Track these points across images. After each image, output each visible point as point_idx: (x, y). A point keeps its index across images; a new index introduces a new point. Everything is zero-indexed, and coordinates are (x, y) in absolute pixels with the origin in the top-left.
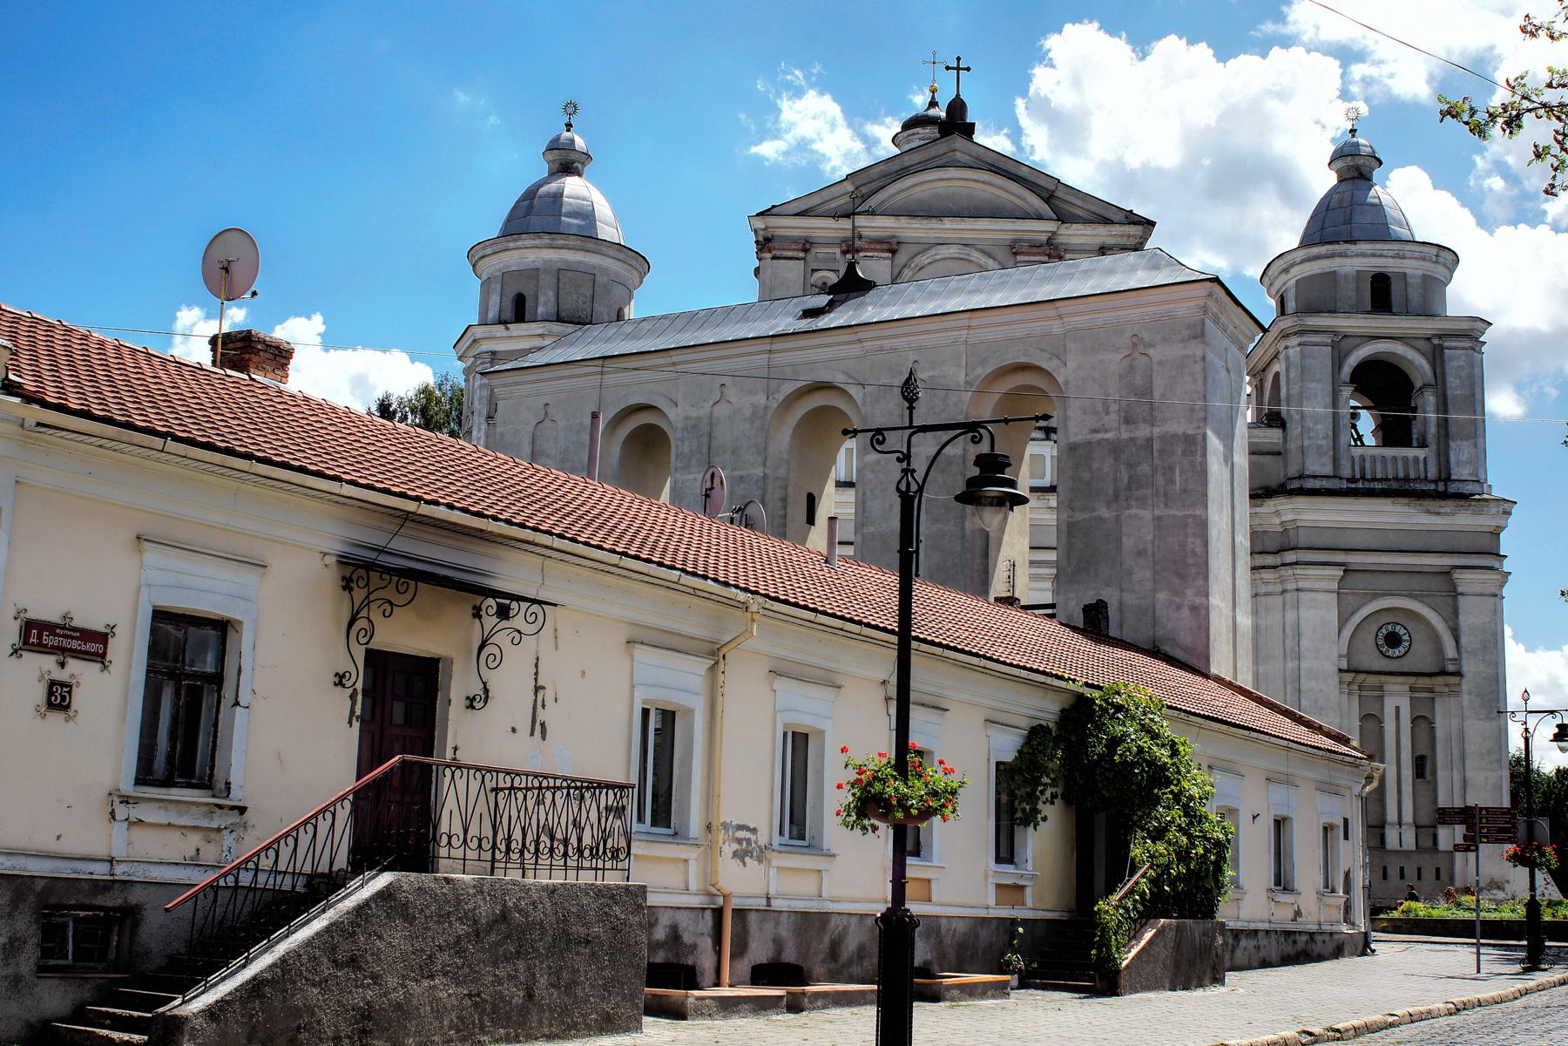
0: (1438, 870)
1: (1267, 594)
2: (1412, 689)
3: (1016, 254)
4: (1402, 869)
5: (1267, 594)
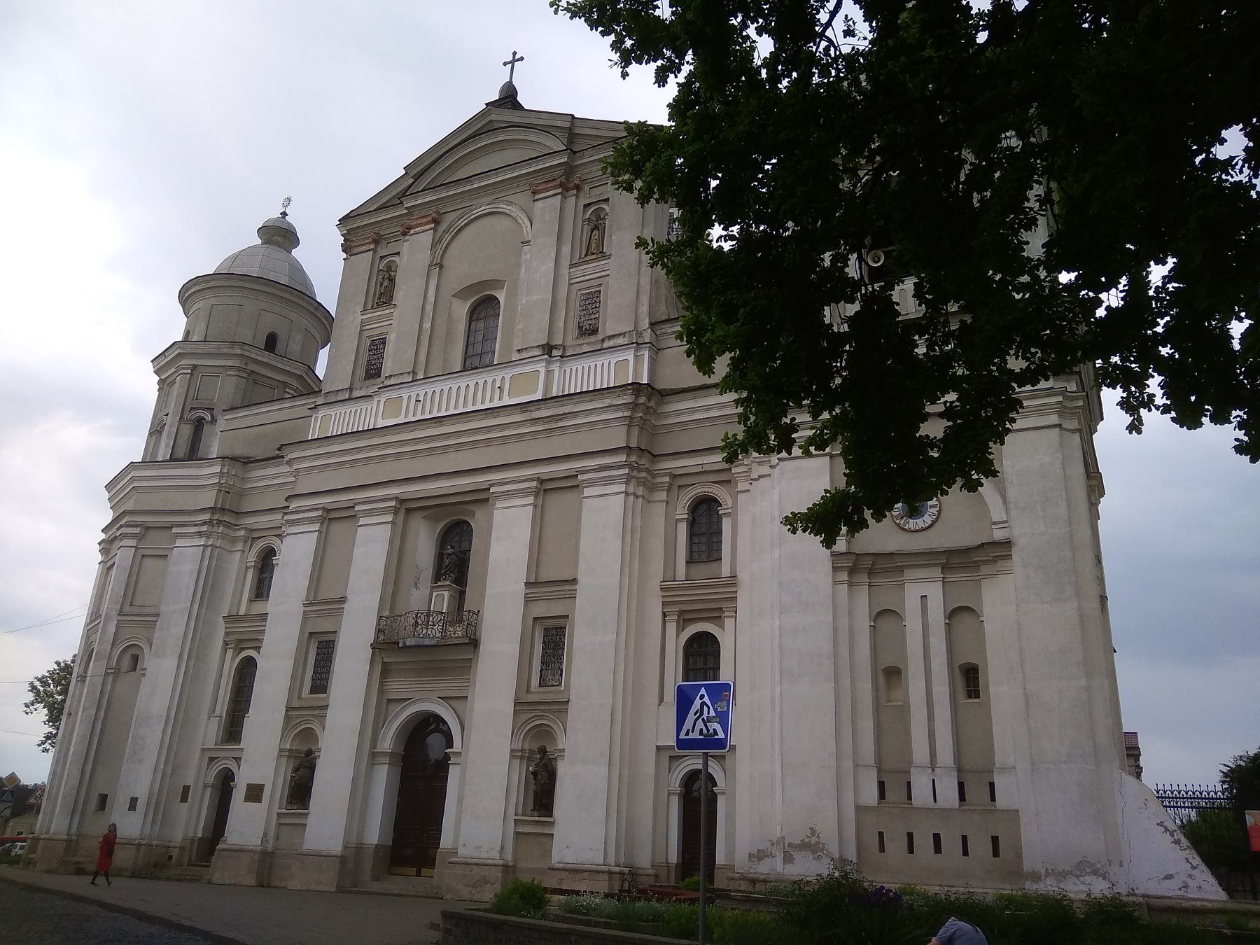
0: (995, 840)
1: (761, 477)
2: (944, 568)
3: (535, 193)
4: (937, 837)
5: (761, 477)
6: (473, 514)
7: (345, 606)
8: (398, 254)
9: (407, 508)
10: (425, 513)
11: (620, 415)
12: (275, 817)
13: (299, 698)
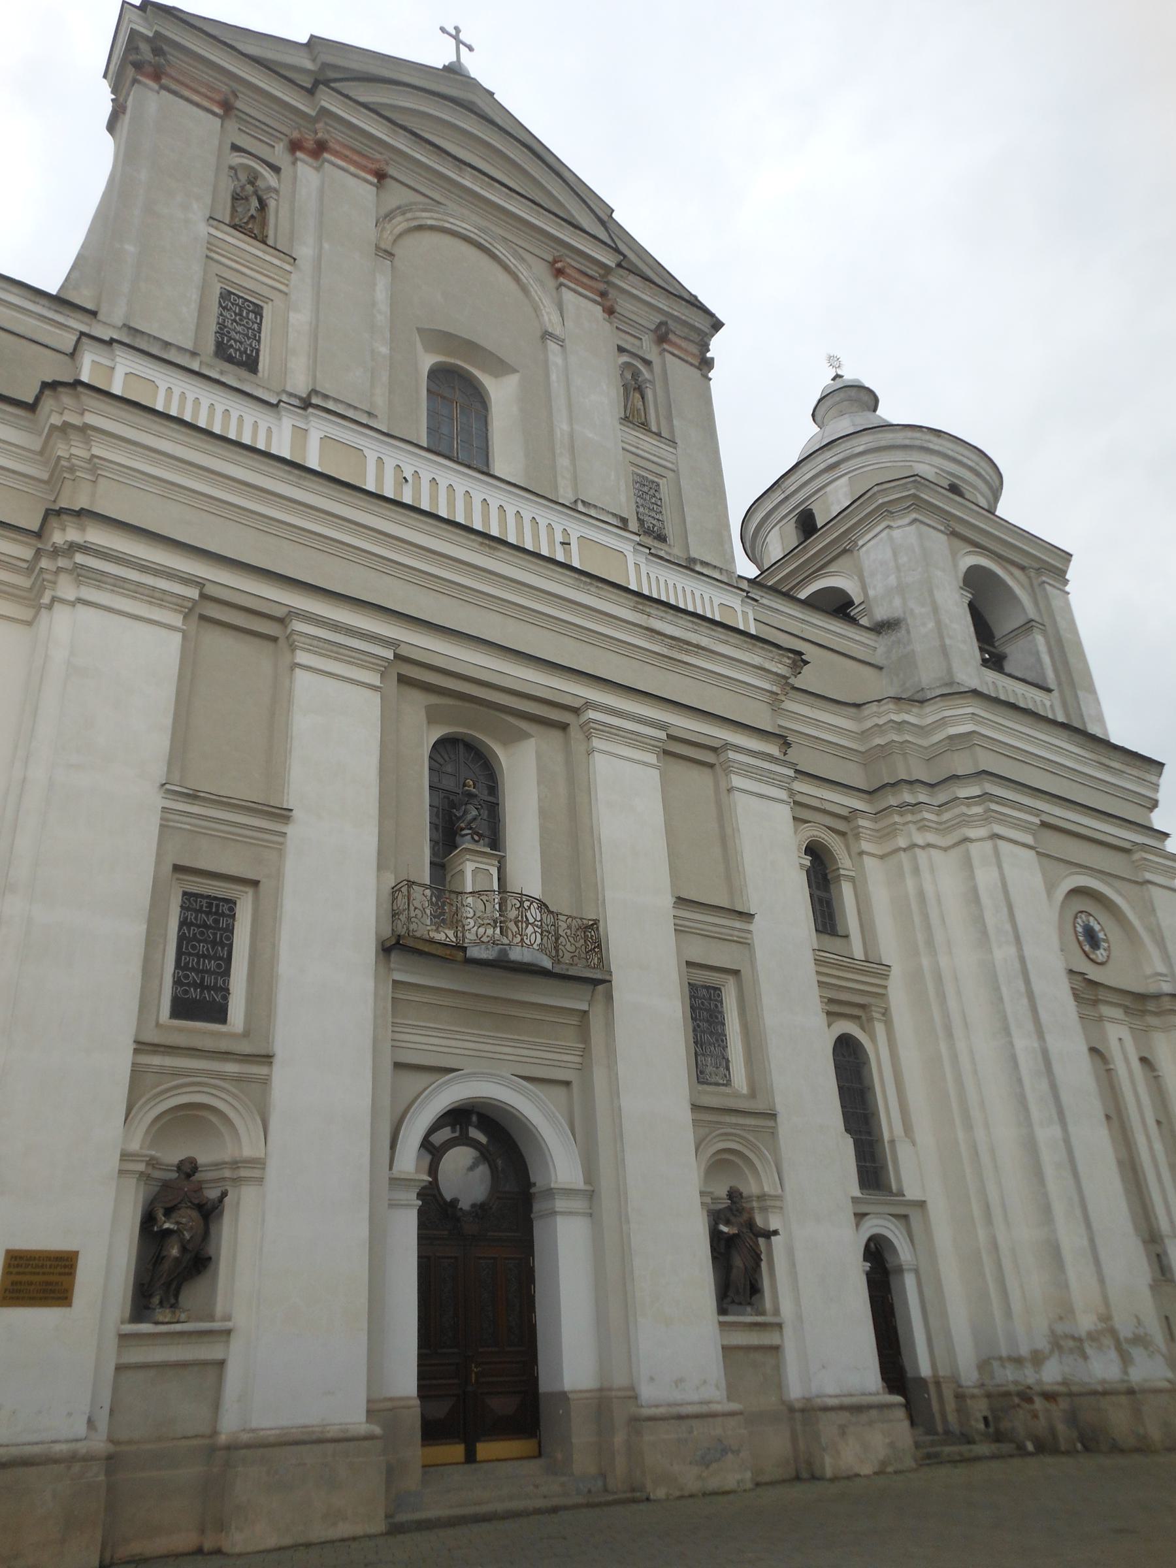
3: (559, 272)
6: (514, 737)
7: (290, 829)
8: (276, 169)
9: (408, 676)
10: (434, 699)
11: (767, 686)
12: (112, 1342)
13: (158, 1025)
